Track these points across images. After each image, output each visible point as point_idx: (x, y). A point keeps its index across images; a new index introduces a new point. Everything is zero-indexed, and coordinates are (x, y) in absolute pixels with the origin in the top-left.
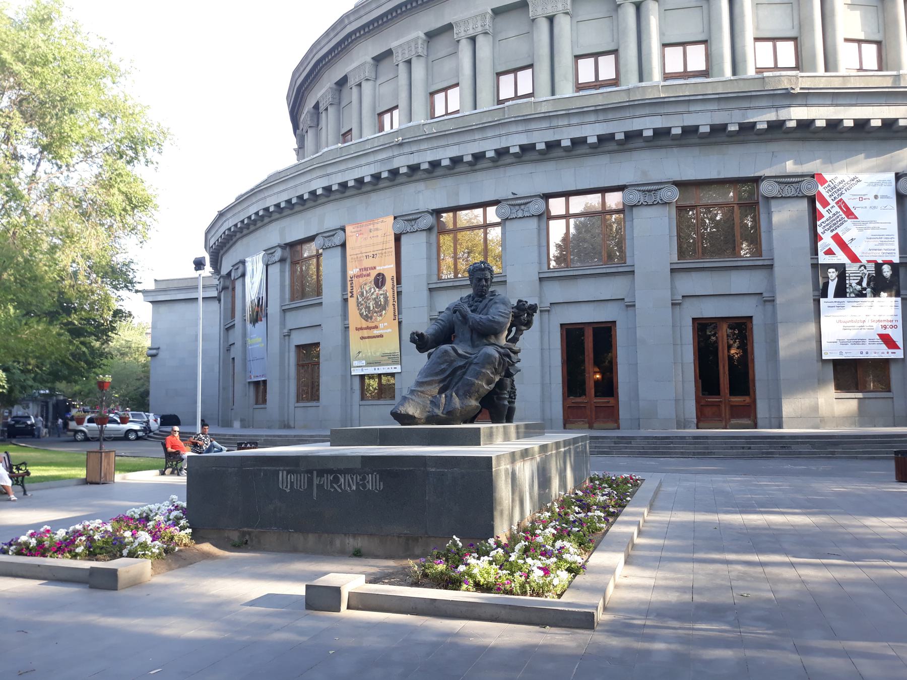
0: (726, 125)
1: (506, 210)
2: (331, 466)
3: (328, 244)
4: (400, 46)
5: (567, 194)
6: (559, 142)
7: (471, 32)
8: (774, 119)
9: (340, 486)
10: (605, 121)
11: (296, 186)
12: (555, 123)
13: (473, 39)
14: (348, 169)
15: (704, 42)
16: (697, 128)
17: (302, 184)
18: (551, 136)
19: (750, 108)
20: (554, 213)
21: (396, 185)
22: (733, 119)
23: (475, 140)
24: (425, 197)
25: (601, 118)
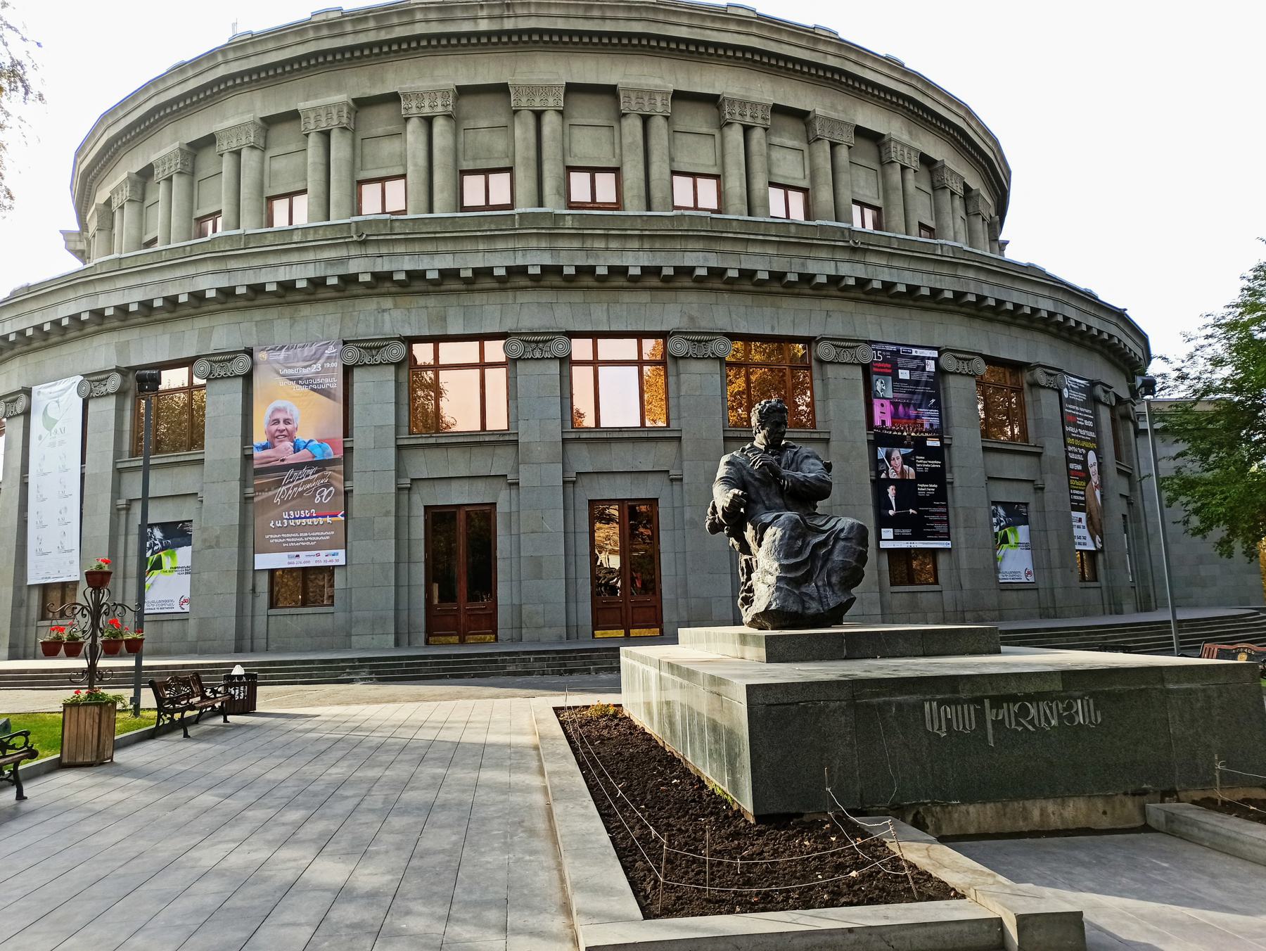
0: (785, 273)
1: (518, 348)
2: (1013, 689)
3: (219, 371)
4: (314, 109)
5: (595, 335)
6: (593, 268)
7: (427, 111)
9: (1031, 722)
10: (652, 250)
11: (163, 282)
12: (588, 244)
13: (428, 121)
14: (266, 266)
16: (755, 272)
17: (176, 279)
19: (809, 258)
20: (576, 356)
21: (347, 298)
22: (793, 267)
23: (478, 251)
24: (393, 318)
25: (646, 246)
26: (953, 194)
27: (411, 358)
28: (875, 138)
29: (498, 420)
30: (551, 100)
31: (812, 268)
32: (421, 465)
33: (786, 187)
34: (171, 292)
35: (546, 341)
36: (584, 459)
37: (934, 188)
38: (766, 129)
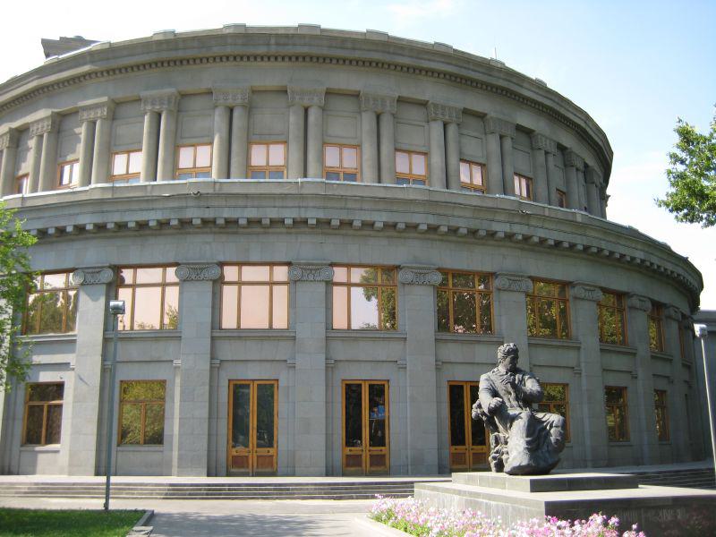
7: (230, 102)
8: (509, 231)
14: (129, 210)
15: (425, 154)
16: (458, 228)
18: (345, 216)
26: (577, 170)
27: (222, 276)
28: (528, 133)
29: (281, 322)
30: (316, 98)
31: (495, 227)
32: (227, 351)
33: (469, 162)
34: (61, 223)
35: (316, 270)
36: (340, 351)
37: (565, 166)
38: (458, 125)
